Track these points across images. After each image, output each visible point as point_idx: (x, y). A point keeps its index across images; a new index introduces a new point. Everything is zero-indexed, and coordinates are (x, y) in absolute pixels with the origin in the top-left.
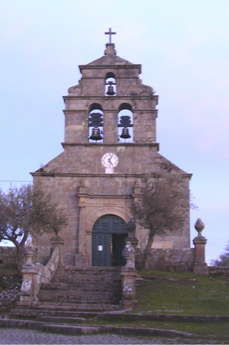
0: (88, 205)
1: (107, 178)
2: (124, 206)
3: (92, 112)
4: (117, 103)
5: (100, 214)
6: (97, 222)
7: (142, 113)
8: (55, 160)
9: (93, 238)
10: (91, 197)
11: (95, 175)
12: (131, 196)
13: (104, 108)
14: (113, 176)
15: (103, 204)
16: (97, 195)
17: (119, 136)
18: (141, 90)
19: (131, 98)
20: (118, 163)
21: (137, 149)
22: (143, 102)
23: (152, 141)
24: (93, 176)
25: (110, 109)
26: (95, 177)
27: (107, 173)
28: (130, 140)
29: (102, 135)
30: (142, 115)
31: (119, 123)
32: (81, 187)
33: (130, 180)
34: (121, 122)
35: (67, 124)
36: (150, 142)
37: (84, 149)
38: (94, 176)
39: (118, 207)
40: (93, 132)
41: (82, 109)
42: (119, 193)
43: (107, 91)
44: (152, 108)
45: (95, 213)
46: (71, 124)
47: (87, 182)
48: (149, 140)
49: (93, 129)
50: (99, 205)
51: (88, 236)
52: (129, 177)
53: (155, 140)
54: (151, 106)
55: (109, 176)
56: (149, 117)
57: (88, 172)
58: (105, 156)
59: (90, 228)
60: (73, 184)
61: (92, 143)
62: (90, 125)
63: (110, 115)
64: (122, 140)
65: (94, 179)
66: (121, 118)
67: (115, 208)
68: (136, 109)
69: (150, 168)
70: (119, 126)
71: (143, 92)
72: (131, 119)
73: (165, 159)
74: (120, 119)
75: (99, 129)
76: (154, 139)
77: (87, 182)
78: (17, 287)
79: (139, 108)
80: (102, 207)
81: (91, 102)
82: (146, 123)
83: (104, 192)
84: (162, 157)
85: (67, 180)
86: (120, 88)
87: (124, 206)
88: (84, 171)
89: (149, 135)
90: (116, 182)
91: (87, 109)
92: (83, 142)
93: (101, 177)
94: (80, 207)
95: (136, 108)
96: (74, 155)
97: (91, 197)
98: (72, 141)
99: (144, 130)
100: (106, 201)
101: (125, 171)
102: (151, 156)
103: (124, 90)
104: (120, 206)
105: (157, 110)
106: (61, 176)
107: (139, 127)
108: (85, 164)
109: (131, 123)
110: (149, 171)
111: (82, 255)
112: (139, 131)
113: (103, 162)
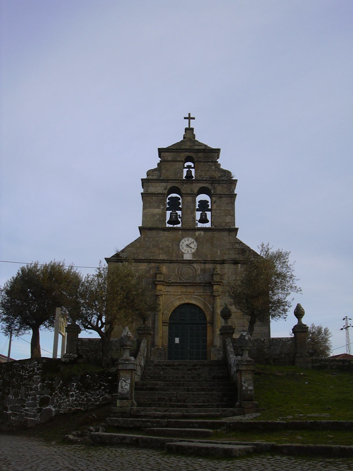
0: (165, 293)
2: (202, 294)
3: (169, 197)
4: (196, 187)
5: (177, 303)
6: (174, 311)
7: (221, 197)
8: (132, 245)
9: (170, 329)
10: (169, 284)
12: (210, 283)
13: (183, 192)
14: (191, 262)
15: (180, 292)
16: (175, 283)
17: (197, 220)
18: (219, 174)
19: (210, 182)
20: (197, 249)
21: (216, 234)
22: (221, 186)
23: (231, 226)
24: (171, 262)
25: (189, 192)
27: (184, 258)
28: (208, 225)
29: (180, 220)
30: (221, 199)
31: (197, 207)
33: (209, 266)
34: (198, 207)
35: (144, 208)
36: (229, 227)
37: (162, 233)
38: (172, 262)
39: (196, 295)
40: (171, 216)
41: (160, 192)
42: (198, 280)
43: (185, 174)
44: (231, 192)
45: (172, 302)
46: (150, 208)
47: (164, 269)
48: (228, 225)
49: (171, 213)
50: (176, 294)
51: (164, 327)
52: (208, 263)
53: (234, 225)
54: (230, 190)
56: (228, 202)
57: (165, 258)
58: (183, 241)
59: (167, 318)
60: (149, 270)
61: (169, 227)
62: (168, 209)
63: (189, 199)
64: (200, 225)
65: (172, 265)
66: (199, 203)
67: (193, 296)
68: (215, 193)
69: (229, 254)
70: (198, 210)
71: (221, 176)
72: (209, 204)
73: (244, 244)
74: (197, 204)
75: (177, 213)
76: (233, 223)
77: (164, 269)
78: (103, 388)
79: (218, 192)
80: (180, 295)
81: (169, 185)
84: (241, 242)
85: (143, 266)
86: (199, 171)
87: (202, 294)
88: (161, 257)
89: (228, 219)
91: (166, 192)
92: (160, 226)
94: (157, 296)
95: (215, 192)
96: (151, 239)
97: (169, 284)
98: (149, 225)
99: (223, 214)
100: (184, 290)
101: (204, 257)
102: (230, 242)
103: (203, 174)
104: (199, 294)
105: (236, 195)
106: (137, 262)
107: (218, 211)
108: (162, 249)
109: (210, 208)
110: (228, 257)
111: (159, 349)
112: (218, 215)
113: (181, 248)
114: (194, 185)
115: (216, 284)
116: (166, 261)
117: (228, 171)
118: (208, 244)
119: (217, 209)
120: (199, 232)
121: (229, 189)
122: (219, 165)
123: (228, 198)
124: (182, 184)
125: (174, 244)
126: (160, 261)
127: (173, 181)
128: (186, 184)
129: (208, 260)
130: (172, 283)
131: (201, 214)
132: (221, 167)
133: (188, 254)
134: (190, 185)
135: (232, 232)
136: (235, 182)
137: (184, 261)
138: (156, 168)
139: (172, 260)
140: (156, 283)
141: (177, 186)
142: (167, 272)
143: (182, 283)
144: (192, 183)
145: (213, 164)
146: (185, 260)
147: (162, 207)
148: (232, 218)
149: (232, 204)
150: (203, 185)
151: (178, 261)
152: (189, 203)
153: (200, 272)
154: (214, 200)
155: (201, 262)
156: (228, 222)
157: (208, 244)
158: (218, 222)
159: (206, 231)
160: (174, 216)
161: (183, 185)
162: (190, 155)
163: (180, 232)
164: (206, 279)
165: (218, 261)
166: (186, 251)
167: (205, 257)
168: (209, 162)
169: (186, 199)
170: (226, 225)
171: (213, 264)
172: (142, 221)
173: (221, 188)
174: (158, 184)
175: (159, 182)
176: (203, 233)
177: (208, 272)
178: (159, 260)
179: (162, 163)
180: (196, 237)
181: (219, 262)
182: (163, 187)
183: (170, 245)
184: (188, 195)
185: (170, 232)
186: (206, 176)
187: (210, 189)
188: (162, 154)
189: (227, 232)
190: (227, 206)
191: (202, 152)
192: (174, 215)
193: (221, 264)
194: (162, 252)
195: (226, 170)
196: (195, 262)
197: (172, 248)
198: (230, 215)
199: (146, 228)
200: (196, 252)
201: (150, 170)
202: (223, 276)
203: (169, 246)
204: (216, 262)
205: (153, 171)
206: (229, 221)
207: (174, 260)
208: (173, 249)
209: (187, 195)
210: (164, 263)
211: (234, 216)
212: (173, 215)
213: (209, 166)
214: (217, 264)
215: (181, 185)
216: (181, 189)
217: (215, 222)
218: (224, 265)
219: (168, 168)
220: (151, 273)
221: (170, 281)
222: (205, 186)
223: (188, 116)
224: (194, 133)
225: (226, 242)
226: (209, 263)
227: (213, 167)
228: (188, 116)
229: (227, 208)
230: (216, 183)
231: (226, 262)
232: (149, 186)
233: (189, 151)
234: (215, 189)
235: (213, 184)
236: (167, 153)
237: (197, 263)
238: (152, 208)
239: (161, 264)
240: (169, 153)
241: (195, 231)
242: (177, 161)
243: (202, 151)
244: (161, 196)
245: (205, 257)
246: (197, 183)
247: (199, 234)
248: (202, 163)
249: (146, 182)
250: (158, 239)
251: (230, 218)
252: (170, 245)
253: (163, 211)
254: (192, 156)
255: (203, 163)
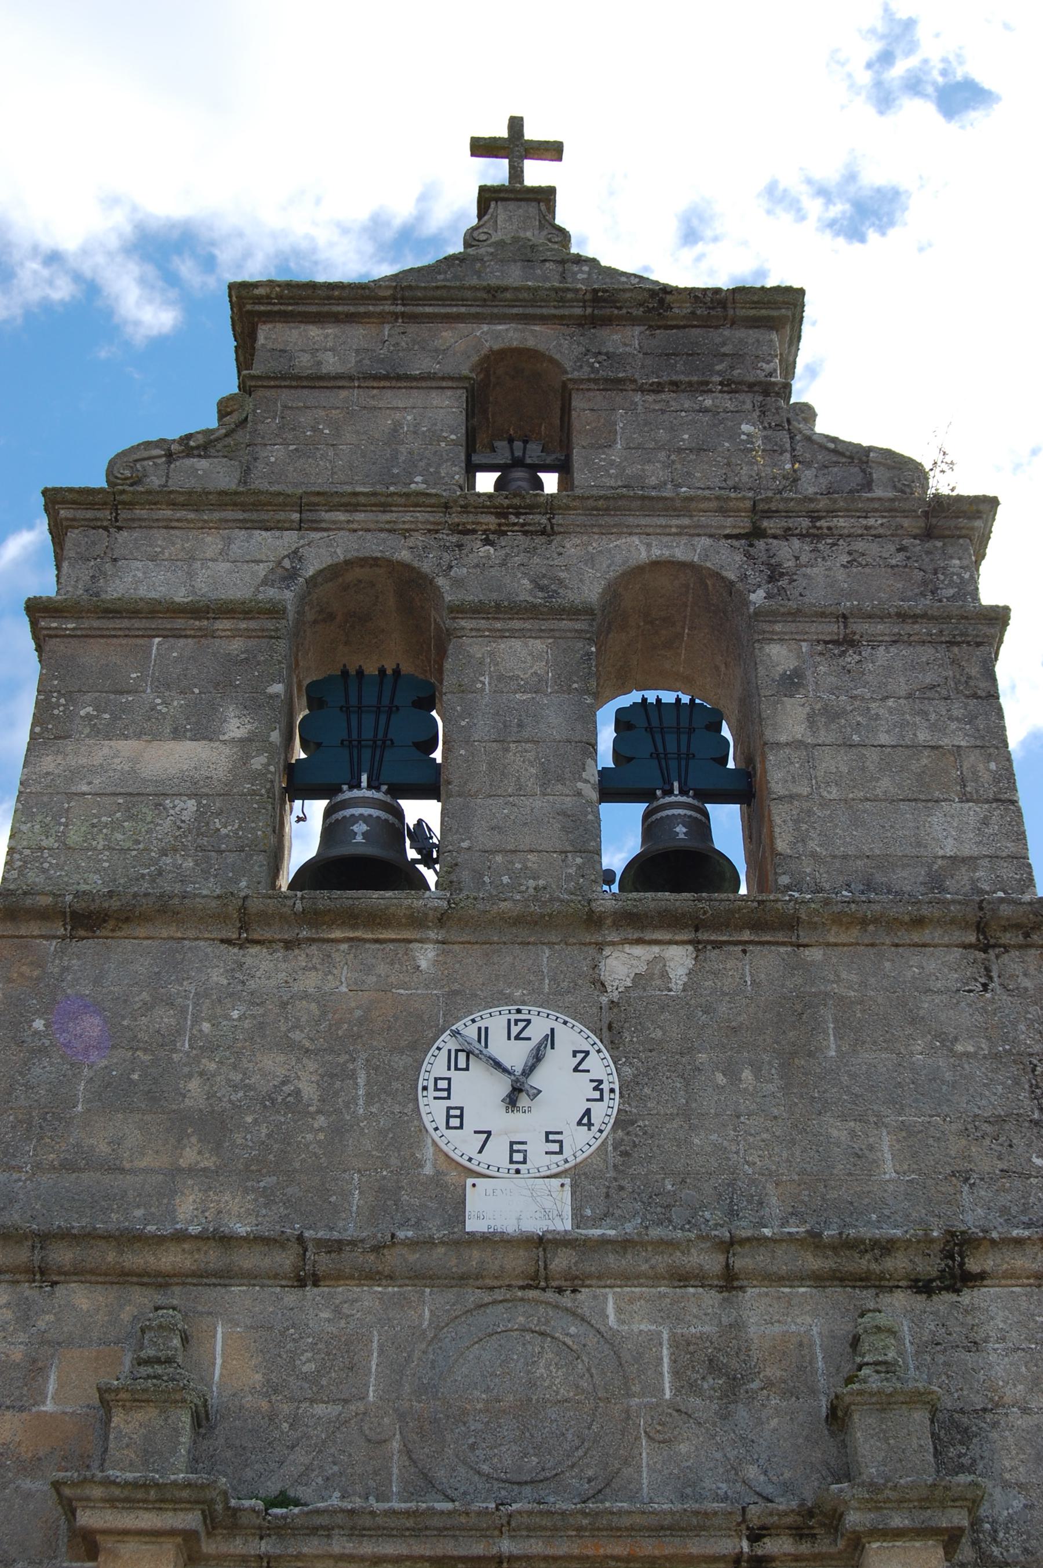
1: (473, 1296)
7: (849, 642)
11: (335, 1247)
14: (561, 1261)
20: (622, 1122)
22: (845, 559)
26: (338, 1277)
32: (138, 1400)
38: (324, 1262)
55: (517, 1261)
56: (929, 679)
79: (817, 596)
82: (903, 725)
83: (440, 1474)
90: (609, 1340)
93: (420, 1277)
107: (831, 762)
112: (834, 793)
114: (572, 547)
115: (898, 1521)
116: (247, 1260)
117: (888, 454)
118: (747, 1075)
119: (823, 736)
120: (638, 950)
121: (919, 575)
122: (807, 412)
123: (927, 653)
124: (454, 539)
125: (353, 1076)
126: (169, 1259)
127: (360, 516)
128: (487, 542)
129: (766, 1239)
130: (314, 1531)
131: (646, 816)
132: (823, 426)
133: (518, 1180)
134: (531, 551)
135: (1015, 953)
136: (978, 523)
137: (475, 1256)
138: (207, 432)
139: (319, 1243)
140: (86, 1519)
141: (405, 555)
142: (253, 1390)
143: (441, 1532)
144: (547, 533)
145: (748, 406)
146: (490, 1241)
147: (236, 727)
148: (985, 822)
149: (975, 696)
150: (656, 552)
151: (393, 1259)
152: (520, 690)
153: (677, 1391)
154: (780, 669)
155: (678, 1258)
156: (953, 859)
157: (747, 1075)
158: (845, 857)
159: (718, 945)
160: (360, 828)
161: (460, 546)
162: (531, 343)
163: (426, 957)
164: (752, 1472)
165: (886, 1247)
166: (497, 1154)
167: (733, 1214)
168: (702, 387)
169: (491, 654)
170: (936, 882)
171: (837, 1293)
172: (11, 851)
173: (840, 575)
174: (212, 542)
175: (223, 524)
176: (690, 963)
177: (769, 1384)
178: (159, 1240)
179: (260, 393)
180: (604, 999)
181: (898, 1263)
182: (258, 562)
183: (309, 1091)
184: (516, 624)
185: (314, 949)
186: (684, 489)
187: (731, 576)
188: (266, 335)
189: (958, 952)
190: (924, 714)
191: (634, 321)
192: (366, 819)
193: (923, 1287)
194: (209, 1162)
195: (870, 449)
196: (611, 1260)
197: (321, 1121)
198: (965, 798)
199: (45, 901)
200: (613, 1157)
201: (148, 445)
202: (966, 1435)
203: (298, 1092)
204: (864, 1263)
205: (170, 456)
206: (967, 850)
207: (353, 1243)
208: (338, 1131)
209: (498, 625)
210: (225, 1277)
211: (1014, 802)
212: (354, 819)
213: (706, 418)
214: (881, 1284)
215: (446, 548)
216: (440, 581)
217: (814, 855)
218: (966, 1298)
219: (314, 429)
220: (49, 1407)
221: (283, 1500)
222: (680, 551)
223: (504, 133)
224: (558, 221)
225: (959, 1048)
226: (781, 1280)
227: (745, 428)
228: (504, 133)
229: (923, 736)
230: (787, 534)
231: (989, 1264)
232: (115, 560)
233: (515, 311)
234: (783, 583)
235: (761, 544)
236: (314, 332)
237: (627, 1278)
238: (126, 738)
239: (176, 1296)
240: (331, 330)
241: (600, 946)
242: (399, 378)
243: (639, 312)
244: (236, 634)
245: (733, 1214)
246: (606, 531)
247: (642, 968)
248: (638, 398)
249: (93, 525)
250: (164, 1018)
251: (972, 820)
252: (309, 1091)
253: (245, 758)
254: (541, 347)
255: (650, 398)
